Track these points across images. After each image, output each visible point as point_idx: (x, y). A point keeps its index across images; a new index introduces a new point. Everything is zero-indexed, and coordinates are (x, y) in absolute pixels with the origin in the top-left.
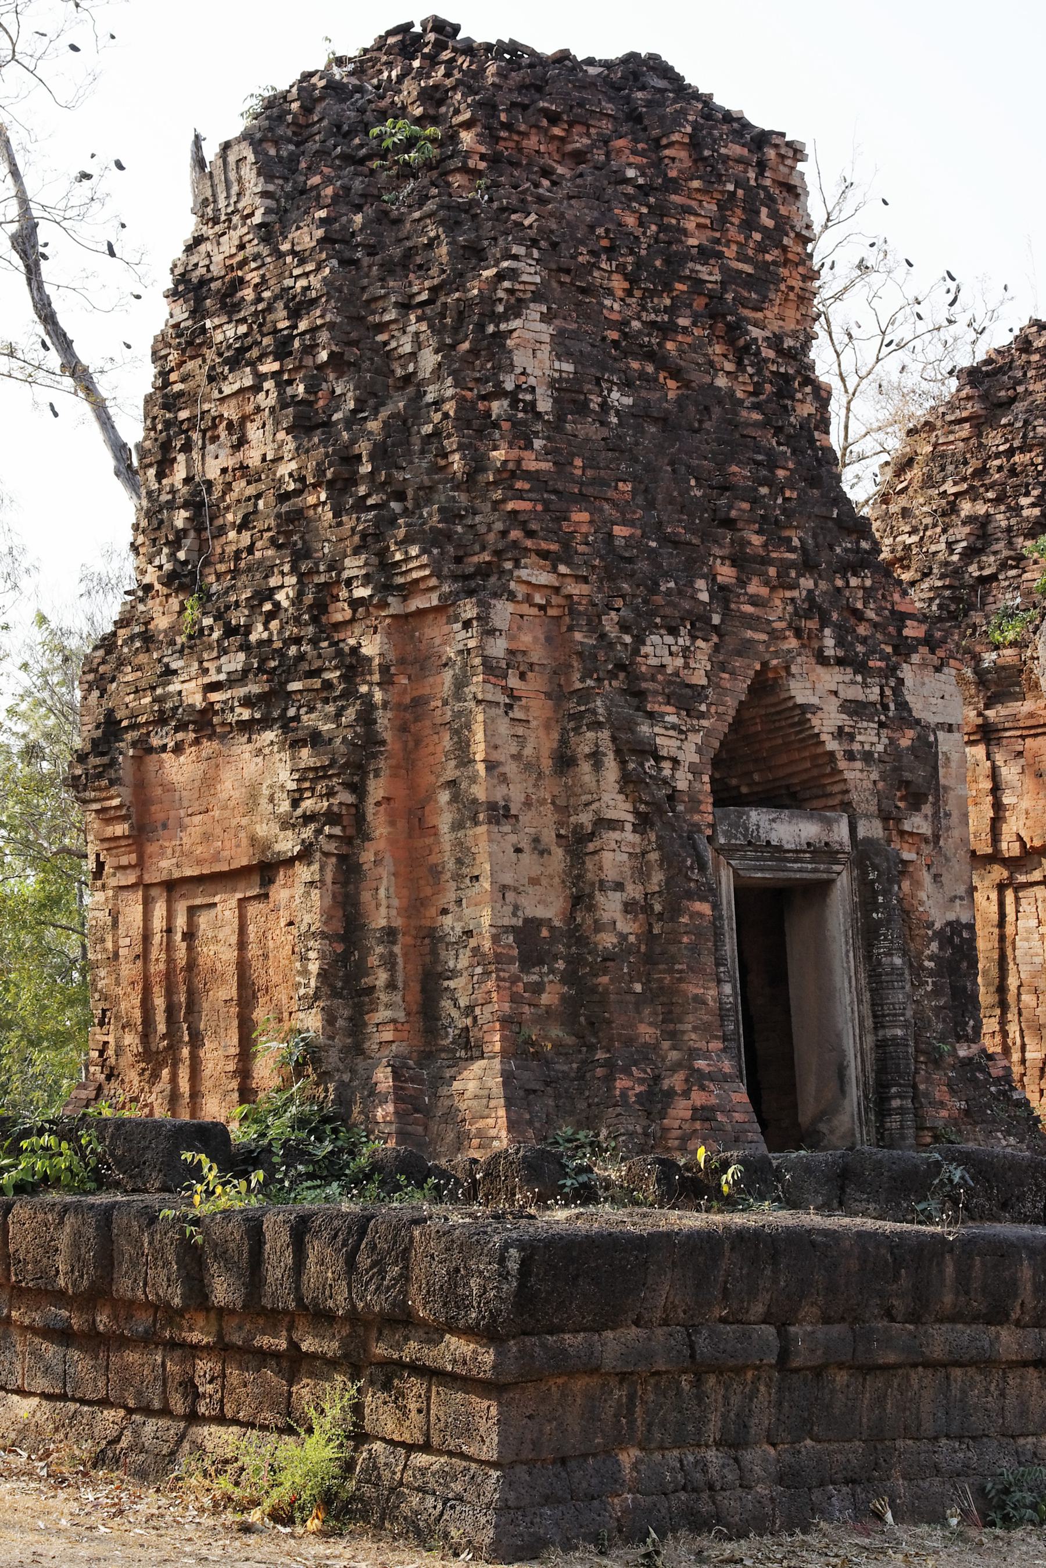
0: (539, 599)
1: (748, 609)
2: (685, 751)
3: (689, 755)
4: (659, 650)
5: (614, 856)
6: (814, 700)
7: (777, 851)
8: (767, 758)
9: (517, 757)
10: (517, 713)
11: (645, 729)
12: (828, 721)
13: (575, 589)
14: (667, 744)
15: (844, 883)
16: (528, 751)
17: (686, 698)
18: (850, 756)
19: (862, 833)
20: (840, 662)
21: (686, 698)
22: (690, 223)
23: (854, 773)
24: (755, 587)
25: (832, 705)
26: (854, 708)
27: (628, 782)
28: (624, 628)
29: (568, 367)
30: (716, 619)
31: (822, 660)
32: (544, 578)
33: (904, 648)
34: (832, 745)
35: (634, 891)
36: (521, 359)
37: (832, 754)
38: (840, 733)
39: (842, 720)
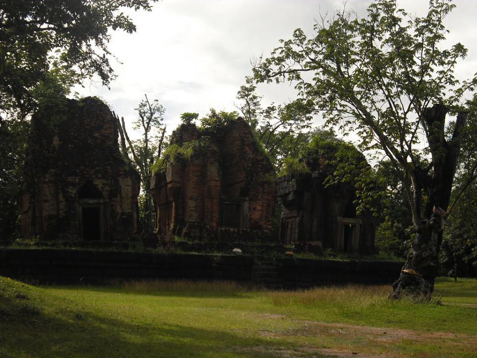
0: (53, 173)
1: (85, 172)
2: (73, 191)
3: (74, 191)
4: (70, 179)
5: (62, 206)
6: (97, 183)
7: (90, 204)
8: (89, 190)
9: (49, 194)
10: (50, 188)
11: (66, 189)
12: (100, 186)
13: (58, 172)
14: (70, 191)
15: (102, 207)
16: (52, 193)
17: (74, 185)
18: (104, 191)
19: (105, 201)
20: (101, 178)
21: (74, 185)
22: (86, 121)
23: (104, 193)
24: (87, 169)
25: (101, 184)
26: (104, 184)
27: (64, 197)
28: (65, 176)
29: (61, 143)
30: (80, 174)
31: (99, 178)
32: (54, 171)
33: (120, 175)
34: (100, 189)
35: (65, 210)
36: (54, 142)
37: (100, 191)
38: (102, 188)
39: (102, 186)
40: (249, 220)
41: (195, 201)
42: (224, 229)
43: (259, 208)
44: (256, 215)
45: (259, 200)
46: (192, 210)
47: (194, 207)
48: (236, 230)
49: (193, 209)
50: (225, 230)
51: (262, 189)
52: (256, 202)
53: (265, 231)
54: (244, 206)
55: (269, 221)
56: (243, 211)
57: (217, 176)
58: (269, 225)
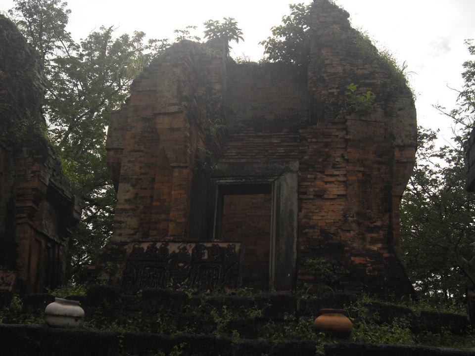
40: (298, 228)
41: (133, 186)
42: (145, 246)
43: (335, 190)
44: (327, 215)
45: (334, 167)
46: (125, 210)
47: (126, 201)
48: (190, 248)
49: (127, 206)
50: (152, 248)
51: (342, 134)
52: (323, 172)
53: (357, 260)
54: (279, 187)
55: (371, 230)
56: (278, 203)
57: (173, 102)
58: (373, 241)
